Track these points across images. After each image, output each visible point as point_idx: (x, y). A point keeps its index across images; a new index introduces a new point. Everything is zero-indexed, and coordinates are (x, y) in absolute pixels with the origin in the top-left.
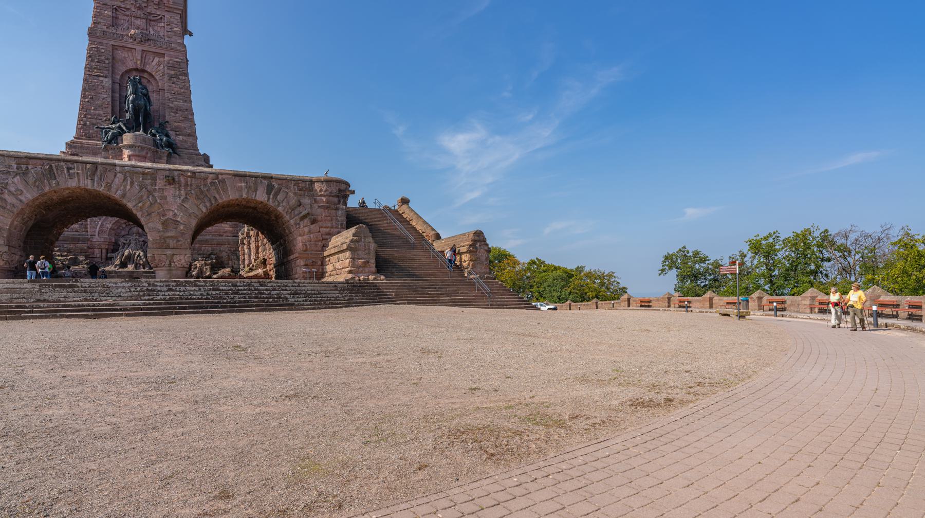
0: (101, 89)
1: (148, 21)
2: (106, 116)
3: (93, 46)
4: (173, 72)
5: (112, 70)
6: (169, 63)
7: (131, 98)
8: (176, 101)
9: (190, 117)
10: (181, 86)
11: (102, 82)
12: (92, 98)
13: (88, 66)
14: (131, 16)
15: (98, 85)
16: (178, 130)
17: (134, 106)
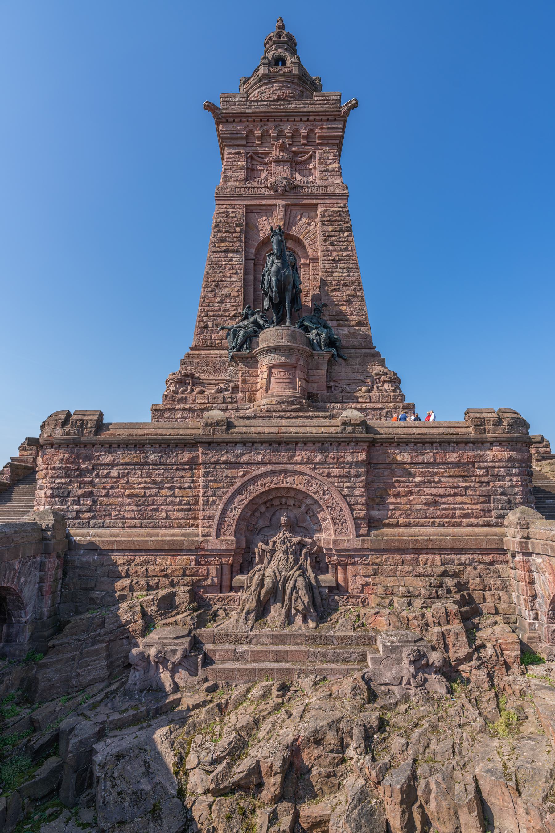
0: (229, 270)
1: (294, 164)
2: (236, 309)
3: (221, 211)
4: (330, 229)
5: (246, 242)
6: (323, 216)
7: (274, 268)
8: (336, 272)
9: (359, 293)
10: (342, 247)
11: (231, 260)
12: (217, 285)
13: (214, 240)
14: (271, 162)
15: (226, 264)
16: (340, 317)
17: (278, 280)
